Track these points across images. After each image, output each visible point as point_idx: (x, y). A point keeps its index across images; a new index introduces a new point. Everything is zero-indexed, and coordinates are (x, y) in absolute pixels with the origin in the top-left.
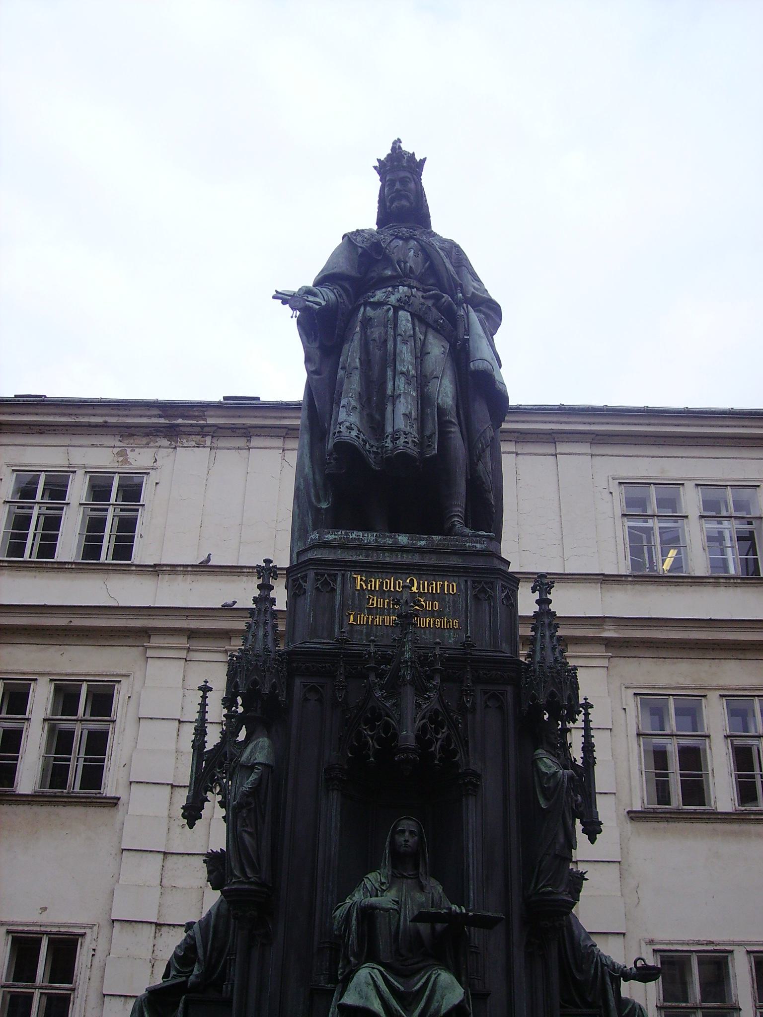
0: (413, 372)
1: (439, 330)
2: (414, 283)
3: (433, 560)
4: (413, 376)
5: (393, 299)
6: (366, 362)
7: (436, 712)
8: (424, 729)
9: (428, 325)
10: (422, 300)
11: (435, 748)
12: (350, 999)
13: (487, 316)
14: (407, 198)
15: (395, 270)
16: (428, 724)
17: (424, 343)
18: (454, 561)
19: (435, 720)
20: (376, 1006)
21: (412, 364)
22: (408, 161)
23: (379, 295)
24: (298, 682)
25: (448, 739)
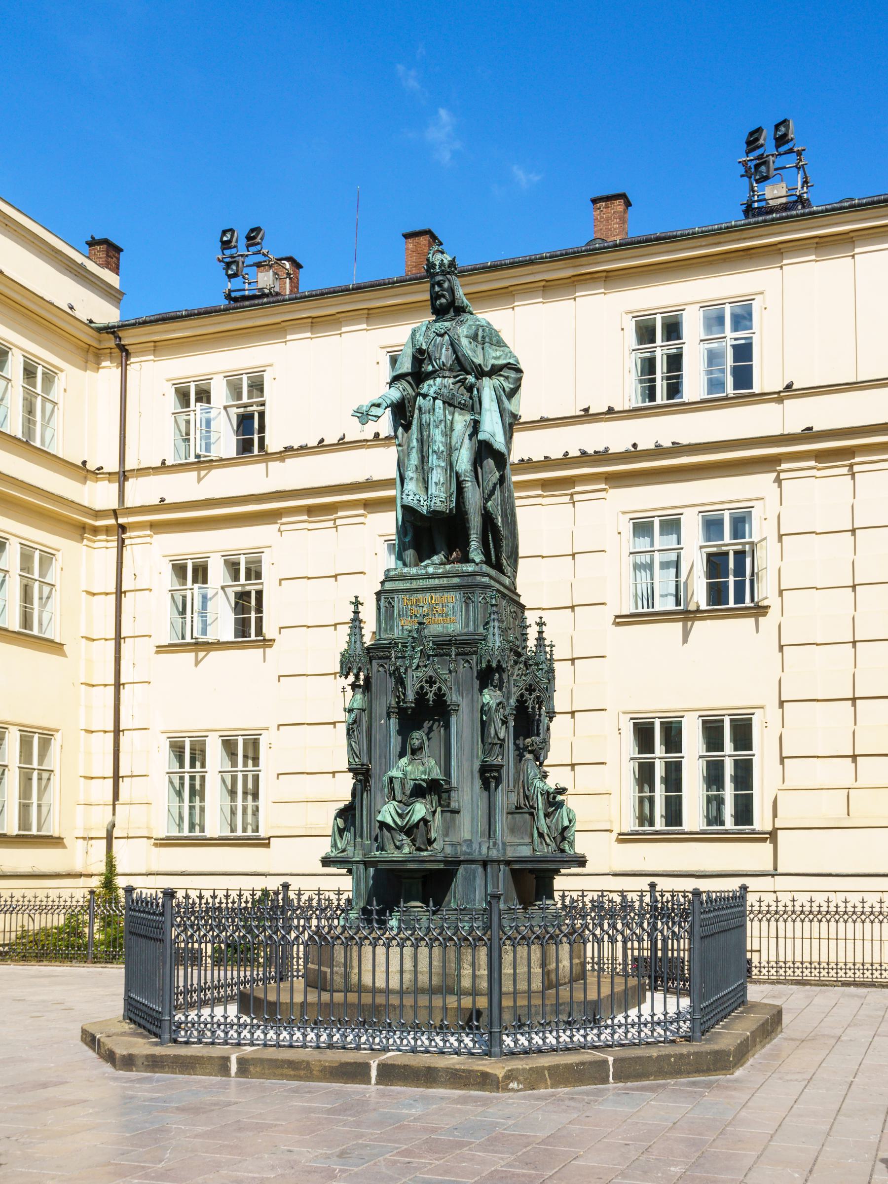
0: (442, 448)
1: (463, 407)
2: (447, 374)
3: (444, 581)
4: (442, 452)
5: (431, 392)
6: (421, 441)
7: (431, 677)
8: (422, 688)
9: (455, 407)
10: (452, 386)
11: (431, 696)
12: (380, 818)
13: (507, 378)
14: (444, 296)
15: (433, 366)
16: (425, 685)
17: (452, 422)
18: (456, 581)
19: (431, 681)
20: (389, 821)
21: (442, 442)
22: (440, 267)
23: (425, 388)
24: (374, 661)
25: (440, 689)
